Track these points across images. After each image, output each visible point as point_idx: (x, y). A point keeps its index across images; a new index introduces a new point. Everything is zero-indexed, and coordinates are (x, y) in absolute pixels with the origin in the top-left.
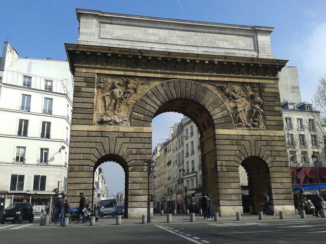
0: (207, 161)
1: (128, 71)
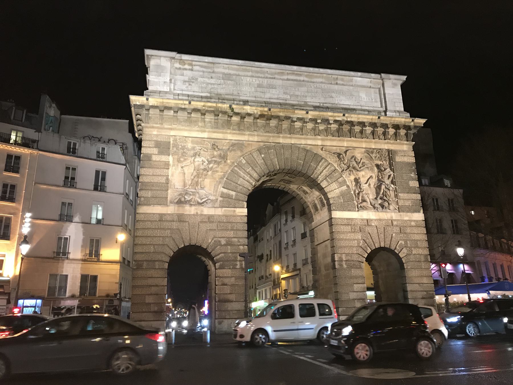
0: (319, 255)
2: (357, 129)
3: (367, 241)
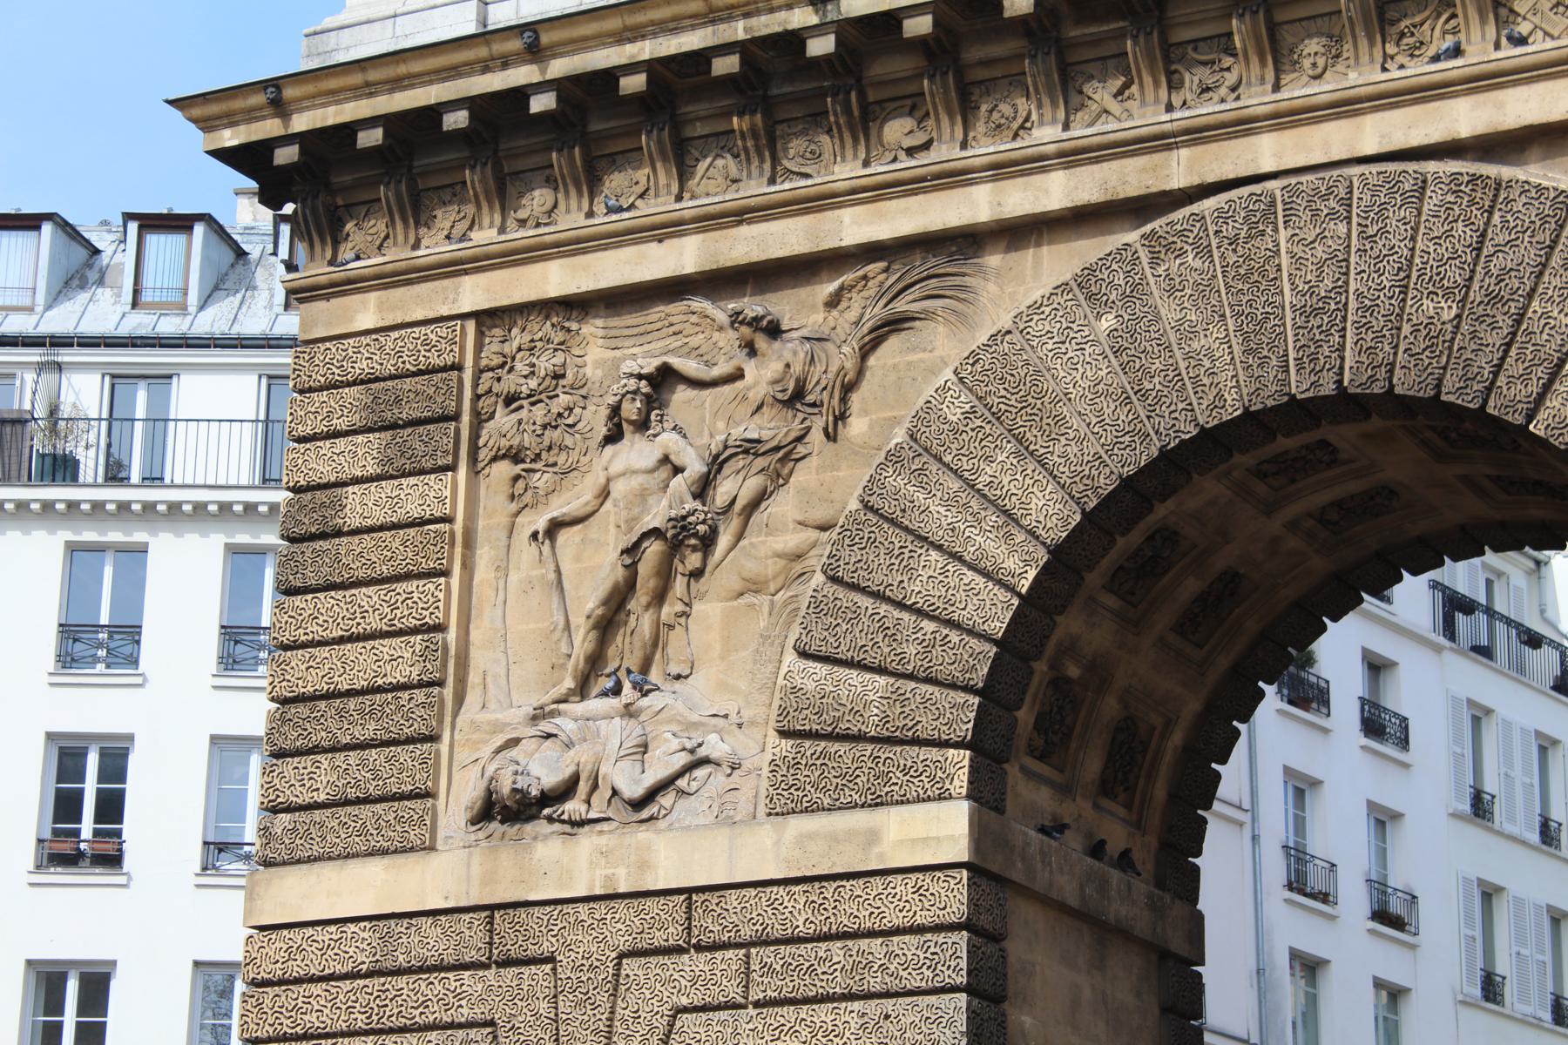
1: (742, 215)
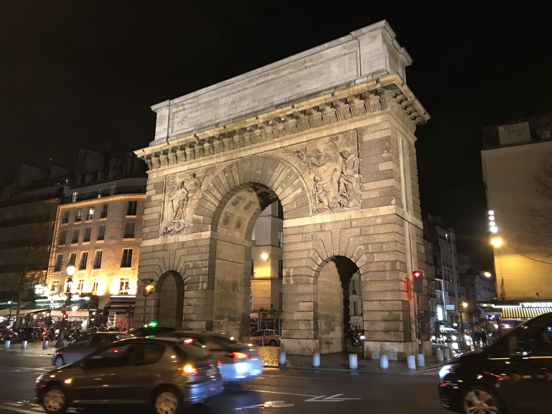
2: (316, 115)
3: (319, 250)
